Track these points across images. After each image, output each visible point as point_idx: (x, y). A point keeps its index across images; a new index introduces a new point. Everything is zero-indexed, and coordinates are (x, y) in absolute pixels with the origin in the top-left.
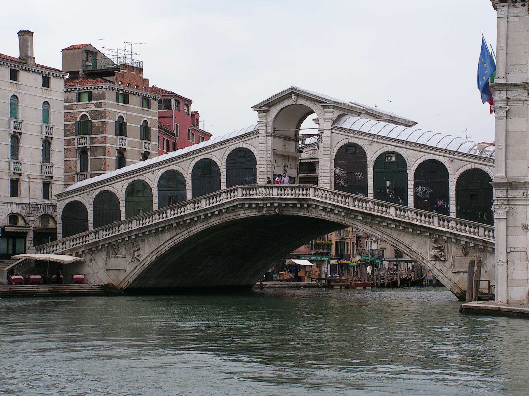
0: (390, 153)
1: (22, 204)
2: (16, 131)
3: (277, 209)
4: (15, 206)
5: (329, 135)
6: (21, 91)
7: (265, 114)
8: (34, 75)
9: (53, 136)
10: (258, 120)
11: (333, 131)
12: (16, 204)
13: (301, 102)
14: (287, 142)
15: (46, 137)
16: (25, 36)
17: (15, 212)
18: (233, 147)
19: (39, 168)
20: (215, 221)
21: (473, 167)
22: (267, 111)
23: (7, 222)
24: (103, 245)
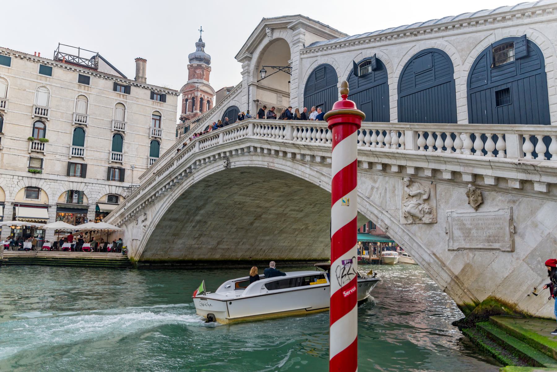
0: (366, 62)
1: (123, 187)
2: (118, 129)
3: (225, 161)
4: (114, 188)
5: (298, 62)
6: (128, 101)
7: (246, 63)
8: (144, 90)
9: (163, 136)
10: (242, 70)
11: (302, 56)
12: (116, 186)
13: (277, 35)
14: (284, 98)
15: (156, 138)
16: (140, 62)
17: (114, 192)
18: (225, 109)
19: (145, 161)
20: (186, 185)
21: (499, 38)
22: (249, 59)
23: (105, 199)
24: (128, 216)
